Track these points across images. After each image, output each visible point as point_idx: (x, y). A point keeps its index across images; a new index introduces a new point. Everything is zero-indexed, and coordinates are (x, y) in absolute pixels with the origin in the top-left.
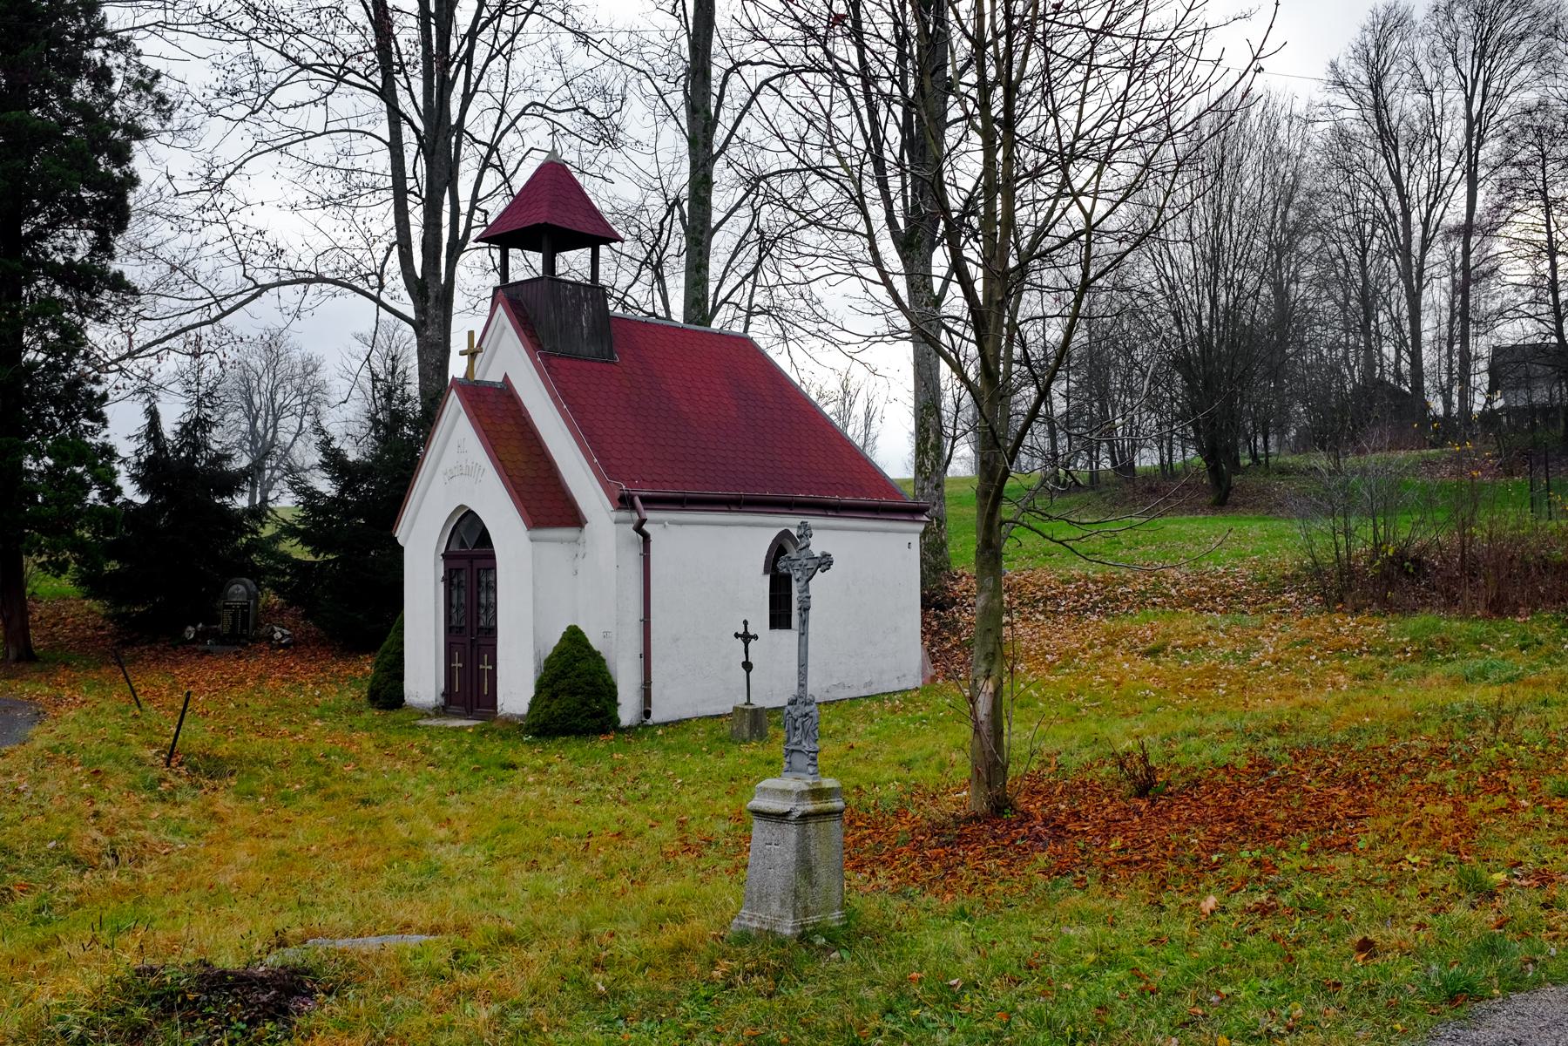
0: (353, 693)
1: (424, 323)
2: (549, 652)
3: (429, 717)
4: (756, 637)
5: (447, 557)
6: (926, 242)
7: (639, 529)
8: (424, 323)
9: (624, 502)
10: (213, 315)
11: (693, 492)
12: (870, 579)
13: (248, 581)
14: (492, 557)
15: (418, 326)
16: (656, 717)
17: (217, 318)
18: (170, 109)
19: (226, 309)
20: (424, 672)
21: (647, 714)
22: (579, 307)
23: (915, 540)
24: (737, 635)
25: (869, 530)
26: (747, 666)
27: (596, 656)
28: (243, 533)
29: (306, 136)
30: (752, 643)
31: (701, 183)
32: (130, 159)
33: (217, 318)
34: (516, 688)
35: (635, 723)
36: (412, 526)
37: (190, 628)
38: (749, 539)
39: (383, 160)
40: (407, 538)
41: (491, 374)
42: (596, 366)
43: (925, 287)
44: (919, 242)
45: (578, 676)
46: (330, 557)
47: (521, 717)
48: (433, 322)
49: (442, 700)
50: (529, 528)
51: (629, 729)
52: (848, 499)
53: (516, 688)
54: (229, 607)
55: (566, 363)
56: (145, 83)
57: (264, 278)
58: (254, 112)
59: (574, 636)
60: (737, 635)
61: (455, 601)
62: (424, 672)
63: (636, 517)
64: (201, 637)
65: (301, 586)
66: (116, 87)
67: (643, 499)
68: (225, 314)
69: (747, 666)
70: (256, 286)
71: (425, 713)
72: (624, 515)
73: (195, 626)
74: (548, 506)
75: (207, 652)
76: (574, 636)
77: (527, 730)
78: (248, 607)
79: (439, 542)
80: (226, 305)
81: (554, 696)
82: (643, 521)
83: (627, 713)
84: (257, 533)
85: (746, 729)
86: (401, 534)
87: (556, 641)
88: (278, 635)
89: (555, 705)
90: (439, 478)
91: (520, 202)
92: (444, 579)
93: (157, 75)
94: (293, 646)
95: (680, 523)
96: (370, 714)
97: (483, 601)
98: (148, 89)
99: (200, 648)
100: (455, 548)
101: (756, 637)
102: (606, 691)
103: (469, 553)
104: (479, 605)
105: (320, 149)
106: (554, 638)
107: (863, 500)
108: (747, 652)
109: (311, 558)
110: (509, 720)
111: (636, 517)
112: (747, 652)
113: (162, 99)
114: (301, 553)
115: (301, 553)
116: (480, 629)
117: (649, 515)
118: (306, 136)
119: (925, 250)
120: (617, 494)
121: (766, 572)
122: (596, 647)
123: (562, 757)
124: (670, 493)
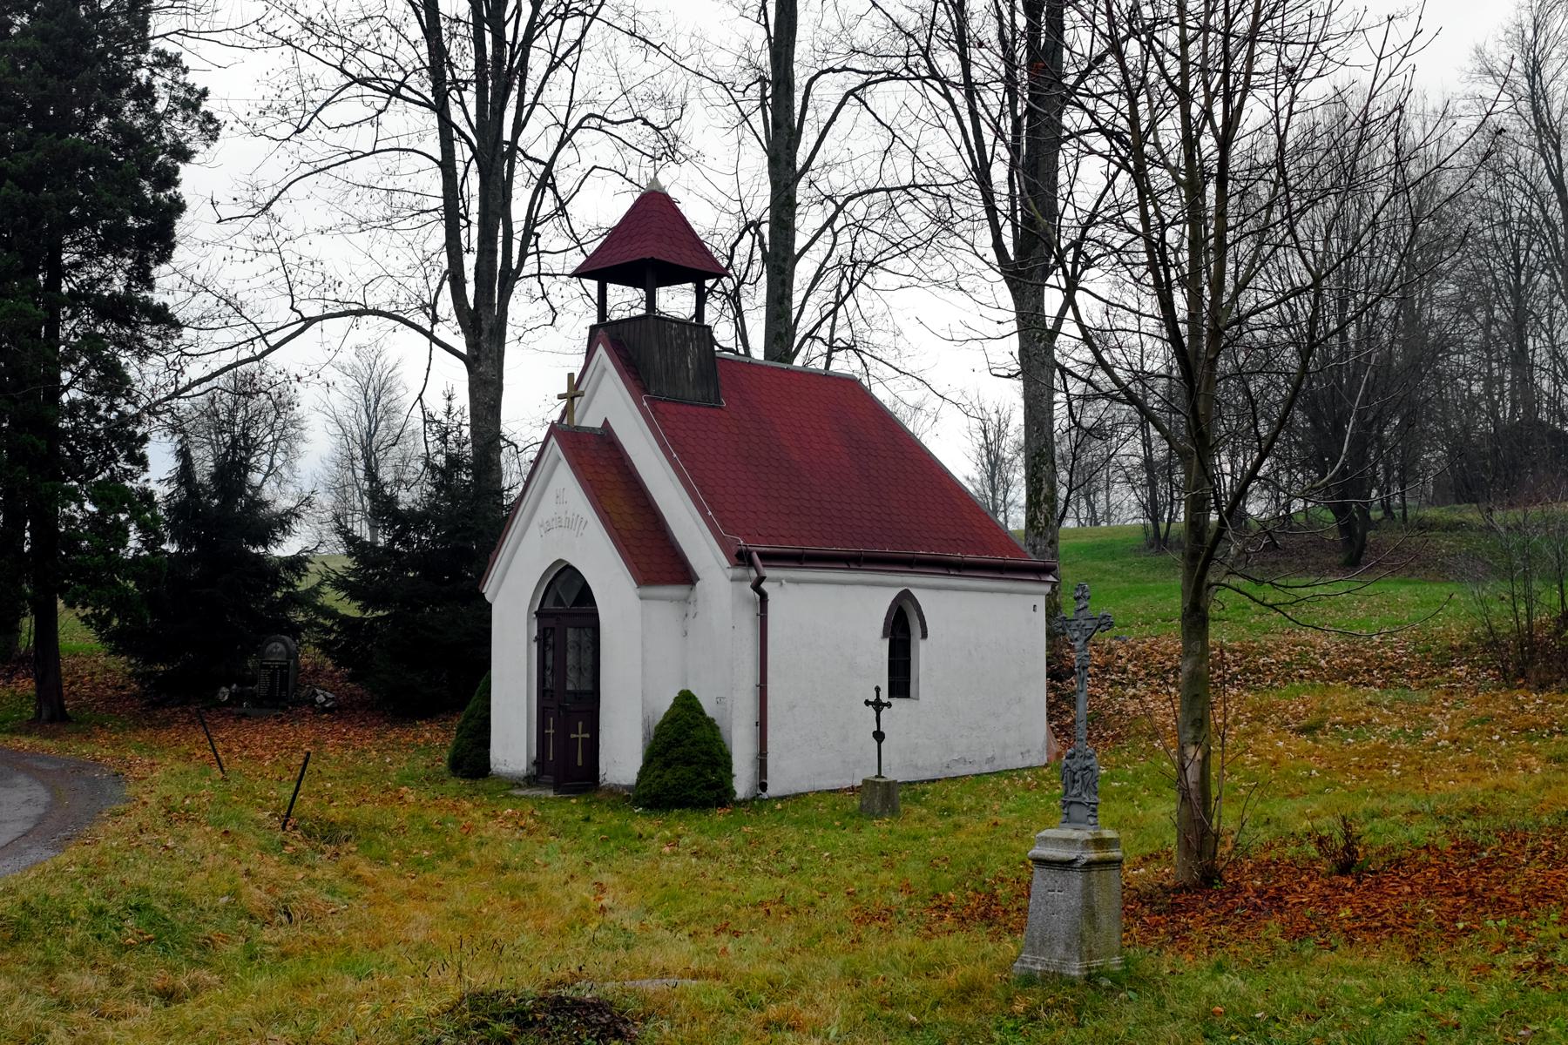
1: (476, 359)
2: (659, 719)
3: (520, 786)
5: (541, 615)
7: (757, 587)
8: (476, 359)
9: (741, 559)
10: (258, 352)
11: (812, 549)
12: (987, 640)
13: (287, 639)
16: (772, 791)
17: (264, 354)
18: (218, 129)
19: (272, 344)
20: (512, 740)
21: (764, 787)
22: (684, 347)
23: (1041, 602)
24: (867, 703)
26: (879, 736)
28: (276, 585)
29: (353, 156)
32: (176, 184)
33: (264, 354)
34: (622, 755)
35: (749, 796)
37: (224, 689)
39: (435, 184)
41: (591, 419)
45: (693, 744)
46: (380, 613)
47: (627, 788)
48: (487, 358)
49: (534, 770)
51: (744, 802)
52: (971, 557)
53: (622, 755)
54: (267, 667)
55: (672, 408)
56: (192, 101)
57: (311, 310)
58: (299, 131)
59: (686, 703)
60: (867, 703)
61: (549, 663)
62: (512, 740)
63: (753, 574)
64: (236, 699)
65: (349, 643)
66: (160, 107)
67: (761, 555)
68: (271, 349)
69: (879, 736)
70: (303, 319)
71: (513, 783)
72: (739, 572)
73: (229, 687)
74: (657, 561)
75: (244, 715)
76: (686, 703)
77: (636, 802)
78: (287, 667)
80: (273, 339)
81: (667, 765)
82: (762, 579)
83: (742, 784)
84: (294, 586)
86: (489, 591)
87: (666, 708)
88: (321, 698)
89: (668, 776)
90: (534, 530)
93: (204, 93)
94: (341, 711)
95: (798, 582)
96: (453, 784)
98: (196, 108)
99: (236, 710)
100: (549, 606)
102: (721, 760)
103: (567, 608)
107: (986, 558)
109: (356, 614)
110: (614, 790)
111: (753, 574)
113: (209, 117)
114: (350, 609)
115: (350, 609)
117: (768, 573)
118: (353, 156)
120: (735, 549)
121: (885, 636)
122: (709, 713)
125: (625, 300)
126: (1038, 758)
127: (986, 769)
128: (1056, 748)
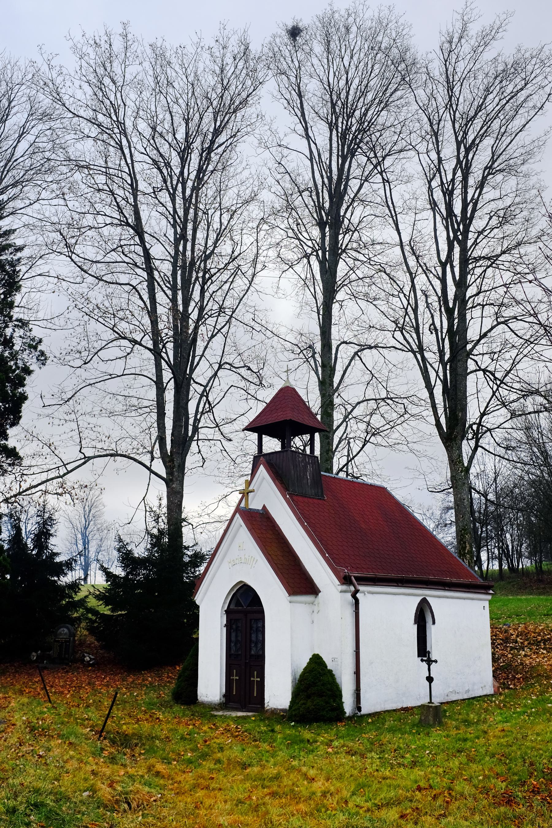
0: (166, 694)
1: (171, 480)
2: (300, 671)
3: (217, 710)
4: (436, 661)
5: (228, 612)
6: (459, 437)
7: (354, 596)
8: (171, 480)
9: (346, 580)
10: (61, 474)
11: (381, 575)
13: (69, 626)
14: (262, 612)
15: (168, 482)
16: (364, 711)
17: (65, 475)
18: (46, 359)
19: (69, 469)
20: (211, 682)
21: (359, 709)
22: (305, 467)
23: (487, 604)
25: (464, 599)
26: (430, 679)
27: (330, 671)
28: (63, 598)
29: (112, 377)
30: (433, 665)
31: (328, 405)
32: (24, 386)
33: (65, 475)
34: (278, 691)
35: (351, 714)
36: (205, 594)
37: (34, 654)
38: (405, 602)
40: (202, 600)
41: (255, 504)
42: (316, 501)
43: (460, 462)
44: (456, 437)
45: (323, 685)
46: (123, 613)
47: (283, 710)
48: (177, 480)
49: (223, 699)
50: (290, 594)
51: (350, 718)
52: (454, 580)
53: (278, 691)
54: (58, 641)
55: (301, 499)
56: (34, 345)
57: (89, 453)
58: (85, 363)
59: (316, 661)
61: (233, 639)
62: (211, 682)
63: (352, 588)
64: (40, 659)
65: (103, 627)
66: (16, 348)
67: (356, 578)
68: (69, 472)
69: (430, 679)
70: (85, 457)
71: (211, 707)
72: (344, 587)
73: (36, 652)
74: (299, 583)
75: (45, 668)
76: (316, 661)
77: (290, 719)
78: (69, 641)
79: (224, 603)
80: (70, 467)
81: (308, 697)
82: (357, 591)
83: (348, 707)
84: (73, 598)
85: (431, 718)
86: (198, 599)
87: (304, 665)
88: (87, 659)
89: (309, 703)
90: (225, 566)
91: (270, 407)
92: (226, 626)
93: (40, 341)
94: (99, 666)
95: (373, 593)
96: (177, 708)
97: (254, 638)
98: (35, 348)
99: (40, 665)
100: (232, 607)
101: (436, 661)
102: (336, 692)
103: (245, 610)
104: (251, 641)
105: (113, 385)
106: (303, 662)
107: (462, 581)
108: (429, 670)
109: (108, 613)
110: (274, 712)
111: (352, 588)
112: (429, 670)
113: (42, 353)
114: (105, 610)
115: (105, 610)
116: (251, 656)
117: (361, 588)
118: (112, 377)
119: (458, 442)
120: (342, 575)
121: (415, 623)
122: (329, 668)
123: (323, 736)
124: (370, 575)
125: (272, 445)
126: (489, 690)
127: (466, 697)
128: (497, 685)
